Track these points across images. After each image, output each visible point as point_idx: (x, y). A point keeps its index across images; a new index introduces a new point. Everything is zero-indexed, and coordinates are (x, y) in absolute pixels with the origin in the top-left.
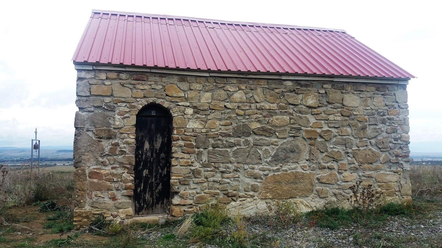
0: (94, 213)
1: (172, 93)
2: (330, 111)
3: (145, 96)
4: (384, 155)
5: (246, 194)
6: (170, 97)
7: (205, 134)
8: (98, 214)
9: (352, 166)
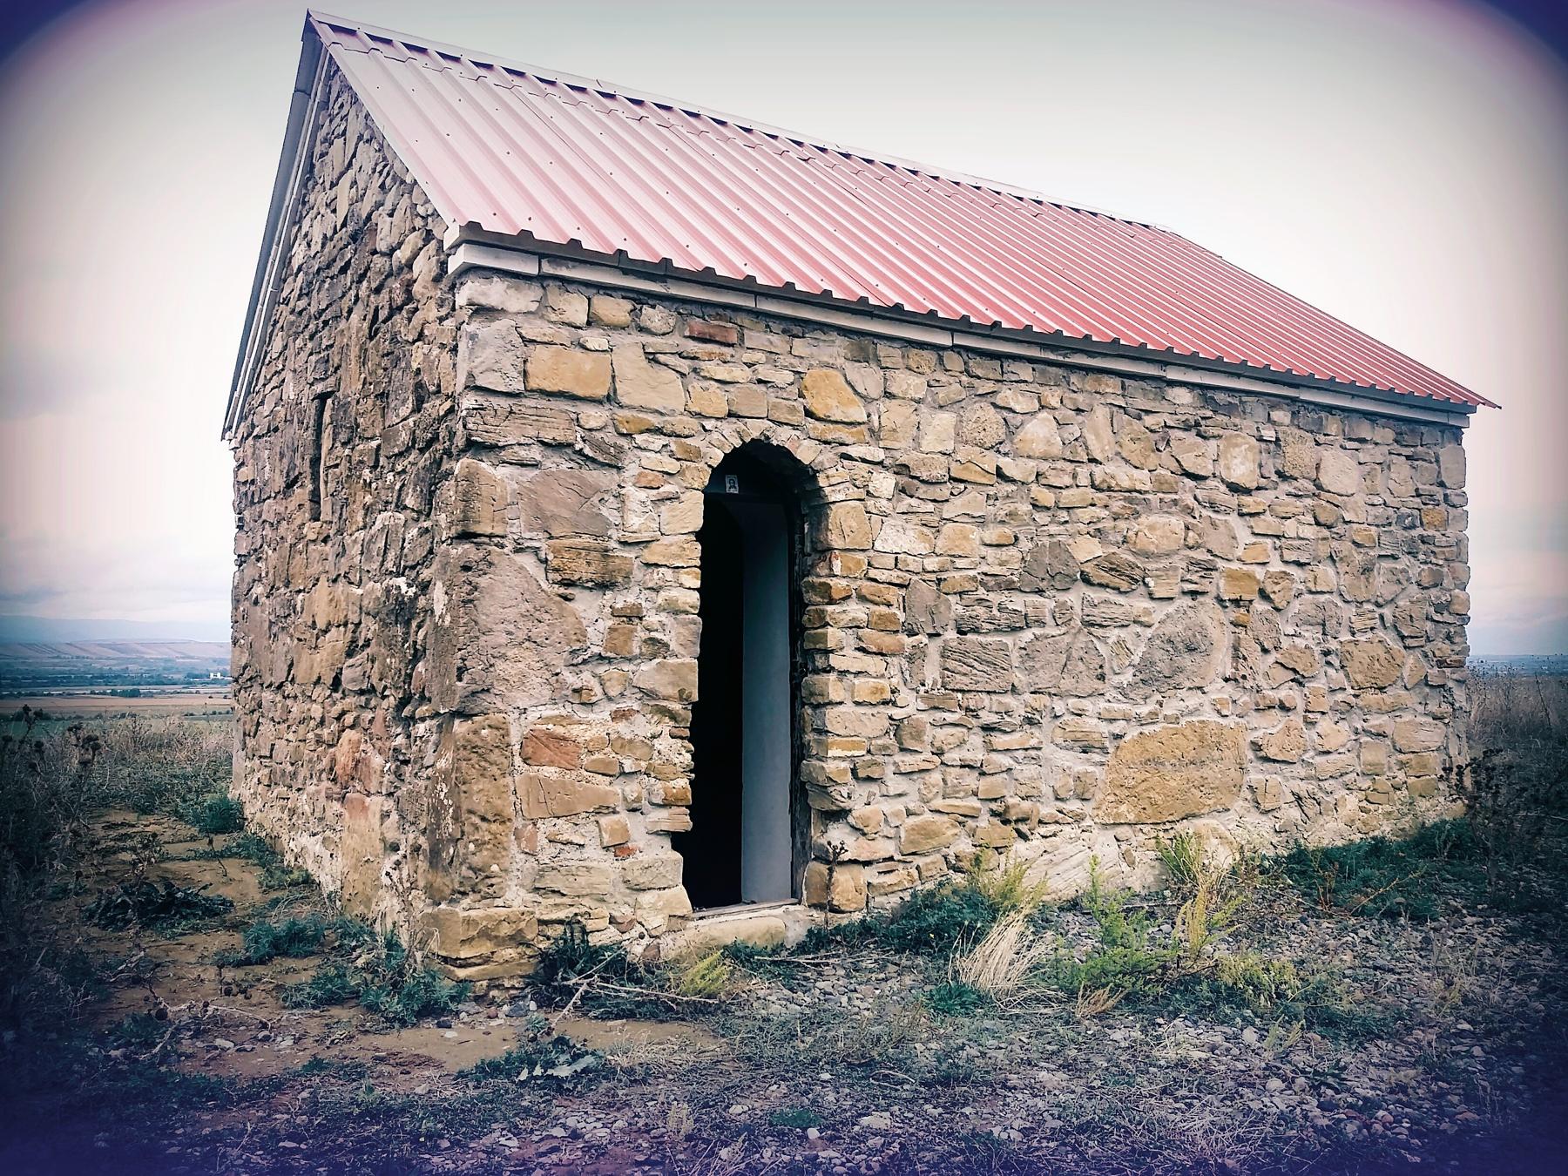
0: (546, 917)
1: (827, 405)
2: (1288, 505)
3: (733, 409)
4: (1410, 661)
5: (1060, 812)
6: (819, 419)
7: (933, 577)
8: (560, 922)
9: (1340, 697)
